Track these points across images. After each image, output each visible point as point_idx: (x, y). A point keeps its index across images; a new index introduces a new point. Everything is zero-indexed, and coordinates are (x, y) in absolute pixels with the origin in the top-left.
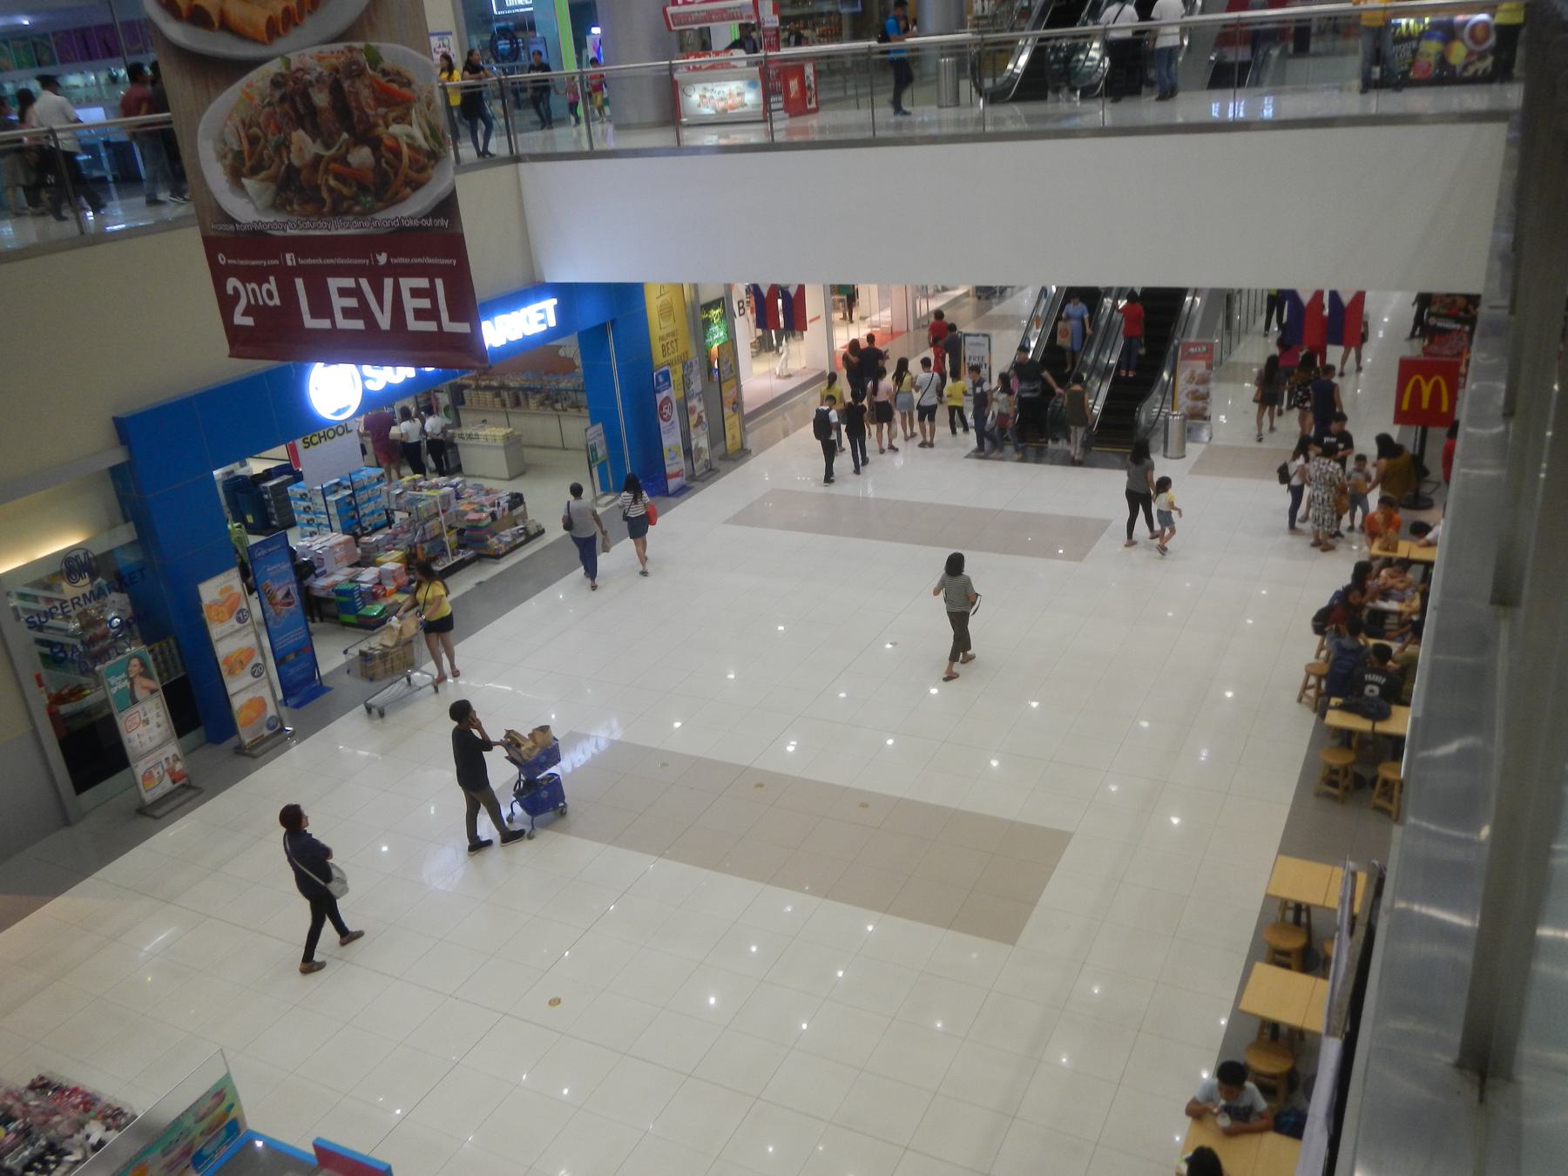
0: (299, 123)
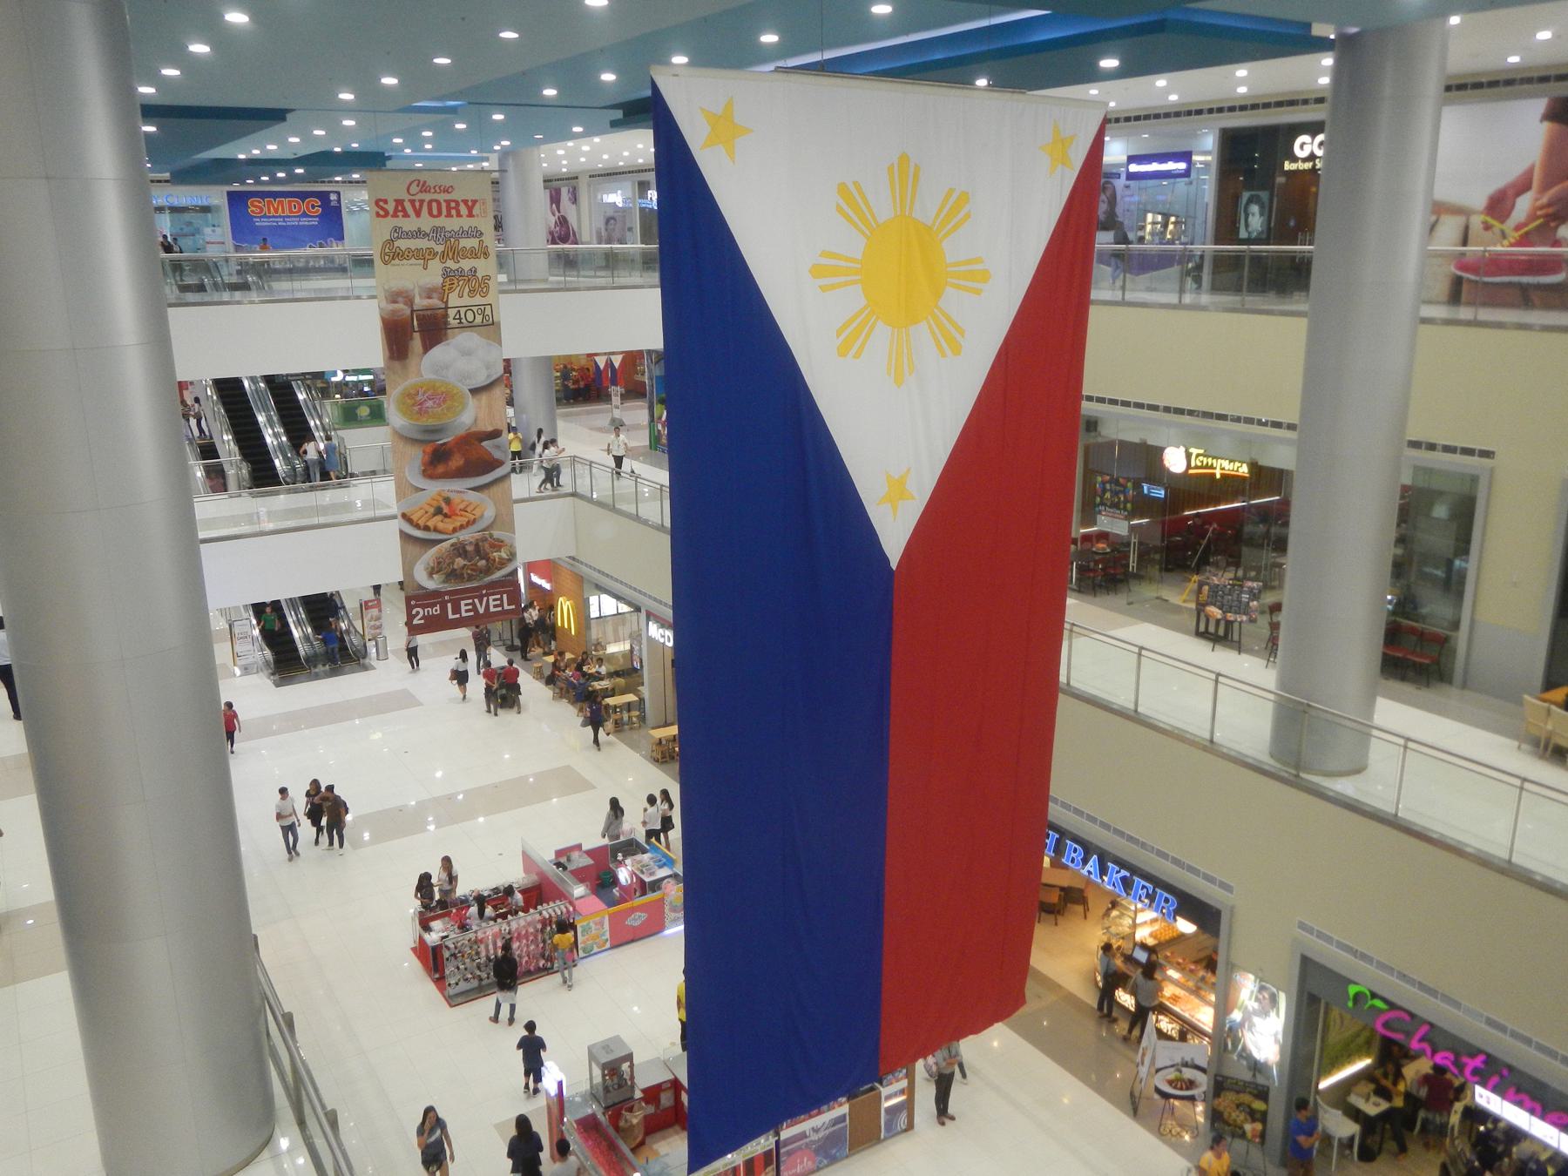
0: (460, 555)
